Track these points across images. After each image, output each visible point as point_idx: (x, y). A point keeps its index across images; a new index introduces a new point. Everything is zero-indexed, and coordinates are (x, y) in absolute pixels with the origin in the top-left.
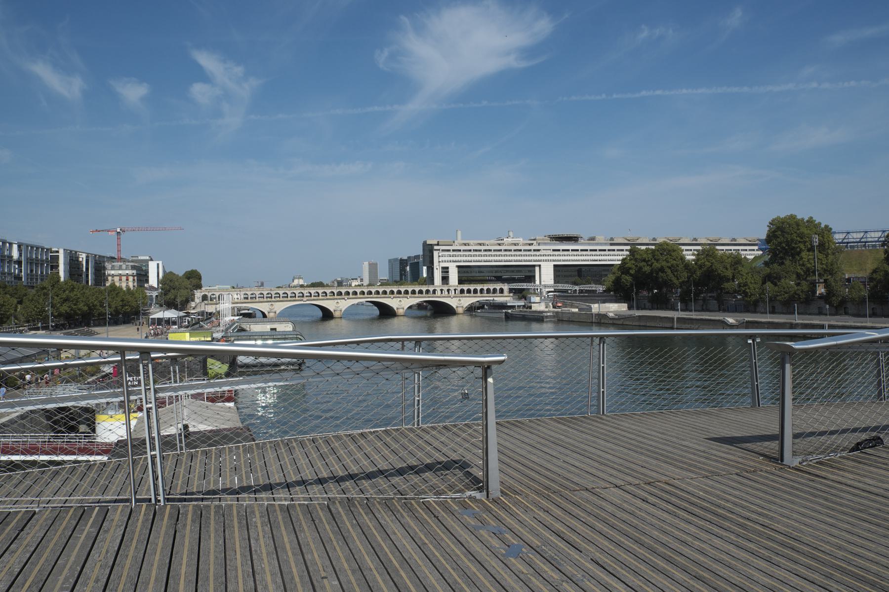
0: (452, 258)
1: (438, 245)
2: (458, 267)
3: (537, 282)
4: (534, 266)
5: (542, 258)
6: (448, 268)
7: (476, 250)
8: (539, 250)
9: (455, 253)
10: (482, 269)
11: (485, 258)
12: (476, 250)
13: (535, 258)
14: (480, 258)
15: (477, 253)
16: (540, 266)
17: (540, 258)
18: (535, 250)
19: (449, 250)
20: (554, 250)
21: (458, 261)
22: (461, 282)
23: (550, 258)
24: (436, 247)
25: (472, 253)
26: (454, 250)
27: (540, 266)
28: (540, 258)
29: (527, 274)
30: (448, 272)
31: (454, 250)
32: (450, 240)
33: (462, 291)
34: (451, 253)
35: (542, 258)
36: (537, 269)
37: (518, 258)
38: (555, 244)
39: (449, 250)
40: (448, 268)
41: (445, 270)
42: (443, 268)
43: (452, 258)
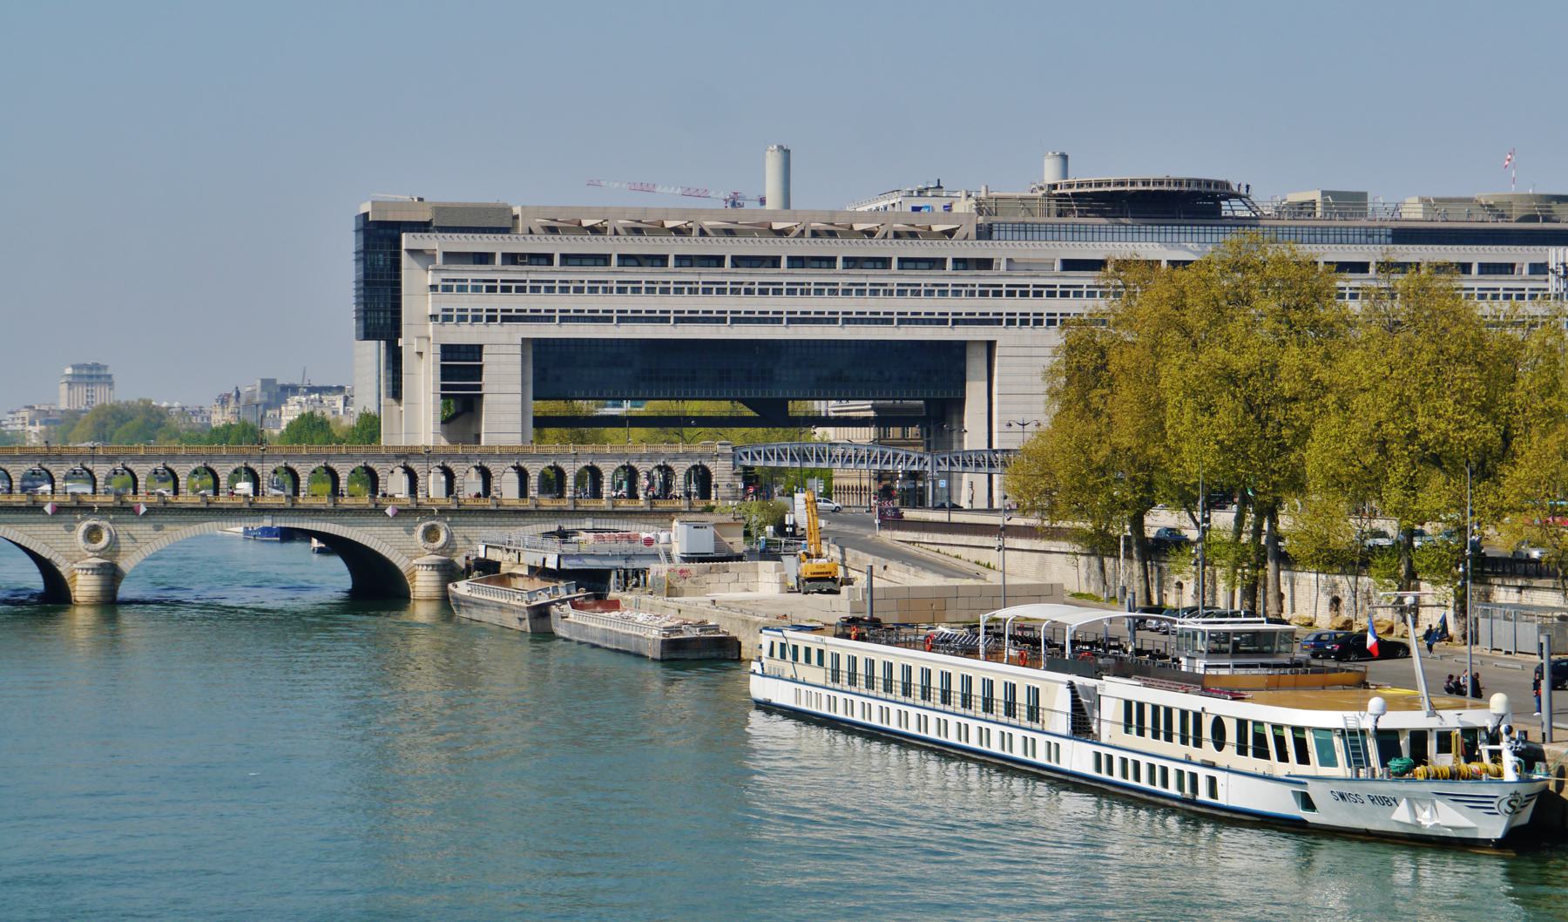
0: (499, 301)
1: (423, 227)
3: (973, 437)
4: (958, 350)
5: (1005, 305)
6: (476, 351)
8: (986, 264)
9: (515, 273)
11: (799, 304)
13: (964, 305)
15: (644, 275)
16: (991, 346)
17: (991, 305)
18: (962, 263)
20: (1069, 265)
21: (535, 318)
23: (1045, 305)
27: (991, 346)
28: (991, 305)
29: (921, 386)
30: (477, 372)
31: (511, 259)
33: (553, 482)
34: (498, 272)
35: (1005, 305)
36: (975, 365)
37: (869, 305)
38: (1076, 232)
39: (484, 258)
40: (476, 351)
41: (461, 367)
42: (448, 351)
43: (499, 301)
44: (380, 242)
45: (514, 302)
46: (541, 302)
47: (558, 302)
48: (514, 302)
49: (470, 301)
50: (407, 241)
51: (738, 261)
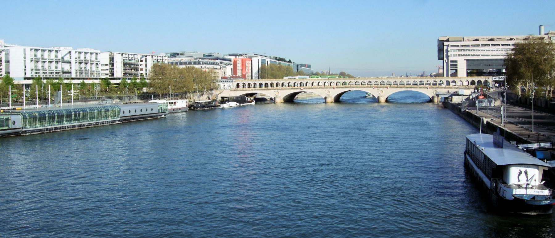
0: (460, 53)
1: (448, 40)
2: (467, 60)
6: (456, 61)
7: (485, 45)
10: (490, 62)
12: (485, 45)
14: (488, 53)
19: (458, 46)
22: (469, 74)
24: (445, 43)
25: (480, 48)
26: (463, 46)
30: (456, 65)
31: (463, 46)
32: (460, 36)
34: (460, 48)
39: (458, 46)
40: (456, 61)
42: (451, 61)
43: (460, 53)
44: (441, 44)
45: (463, 53)
46: (468, 53)
47: (470, 53)
48: (463, 53)
49: (455, 53)
50: (445, 43)
51: (503, 45)
